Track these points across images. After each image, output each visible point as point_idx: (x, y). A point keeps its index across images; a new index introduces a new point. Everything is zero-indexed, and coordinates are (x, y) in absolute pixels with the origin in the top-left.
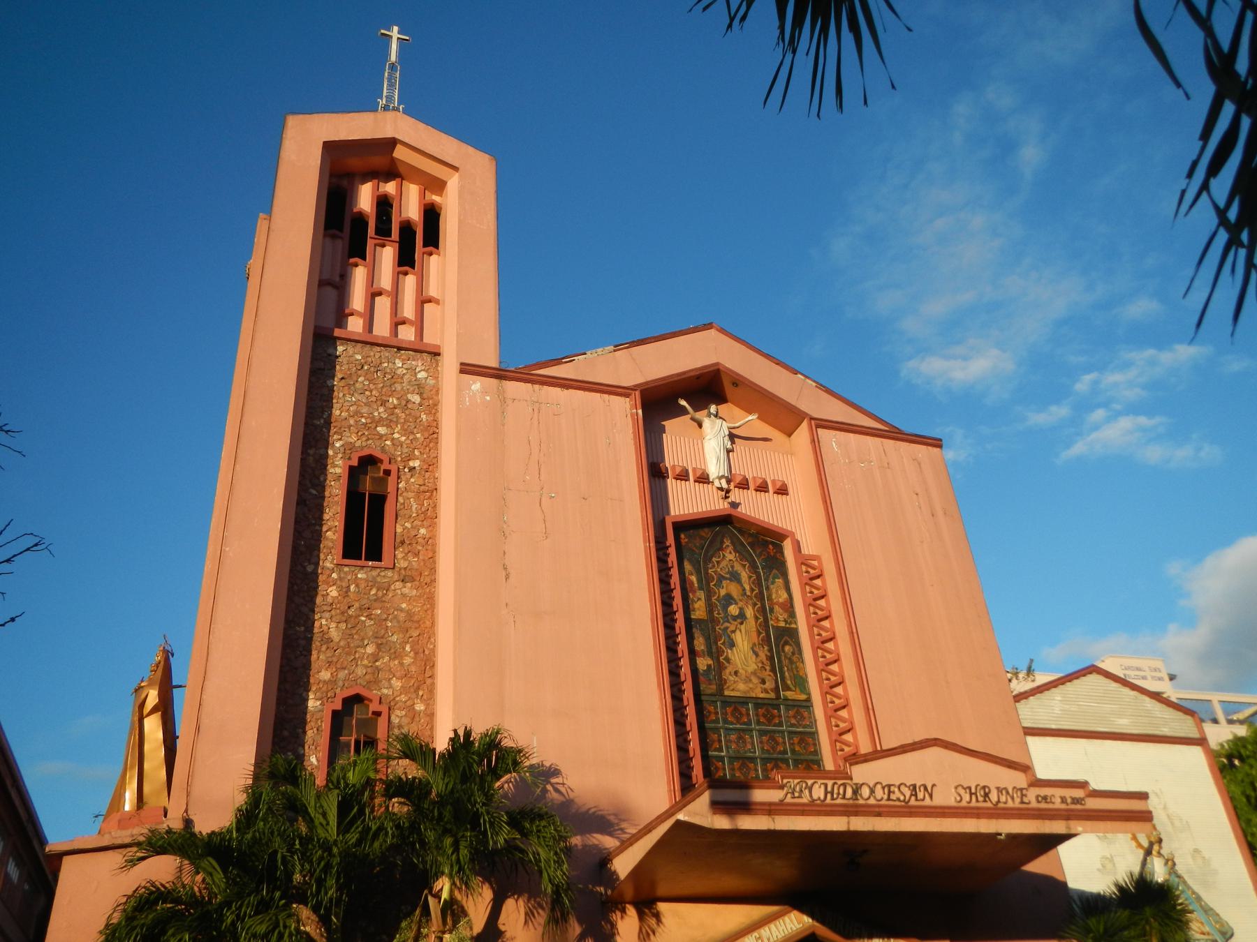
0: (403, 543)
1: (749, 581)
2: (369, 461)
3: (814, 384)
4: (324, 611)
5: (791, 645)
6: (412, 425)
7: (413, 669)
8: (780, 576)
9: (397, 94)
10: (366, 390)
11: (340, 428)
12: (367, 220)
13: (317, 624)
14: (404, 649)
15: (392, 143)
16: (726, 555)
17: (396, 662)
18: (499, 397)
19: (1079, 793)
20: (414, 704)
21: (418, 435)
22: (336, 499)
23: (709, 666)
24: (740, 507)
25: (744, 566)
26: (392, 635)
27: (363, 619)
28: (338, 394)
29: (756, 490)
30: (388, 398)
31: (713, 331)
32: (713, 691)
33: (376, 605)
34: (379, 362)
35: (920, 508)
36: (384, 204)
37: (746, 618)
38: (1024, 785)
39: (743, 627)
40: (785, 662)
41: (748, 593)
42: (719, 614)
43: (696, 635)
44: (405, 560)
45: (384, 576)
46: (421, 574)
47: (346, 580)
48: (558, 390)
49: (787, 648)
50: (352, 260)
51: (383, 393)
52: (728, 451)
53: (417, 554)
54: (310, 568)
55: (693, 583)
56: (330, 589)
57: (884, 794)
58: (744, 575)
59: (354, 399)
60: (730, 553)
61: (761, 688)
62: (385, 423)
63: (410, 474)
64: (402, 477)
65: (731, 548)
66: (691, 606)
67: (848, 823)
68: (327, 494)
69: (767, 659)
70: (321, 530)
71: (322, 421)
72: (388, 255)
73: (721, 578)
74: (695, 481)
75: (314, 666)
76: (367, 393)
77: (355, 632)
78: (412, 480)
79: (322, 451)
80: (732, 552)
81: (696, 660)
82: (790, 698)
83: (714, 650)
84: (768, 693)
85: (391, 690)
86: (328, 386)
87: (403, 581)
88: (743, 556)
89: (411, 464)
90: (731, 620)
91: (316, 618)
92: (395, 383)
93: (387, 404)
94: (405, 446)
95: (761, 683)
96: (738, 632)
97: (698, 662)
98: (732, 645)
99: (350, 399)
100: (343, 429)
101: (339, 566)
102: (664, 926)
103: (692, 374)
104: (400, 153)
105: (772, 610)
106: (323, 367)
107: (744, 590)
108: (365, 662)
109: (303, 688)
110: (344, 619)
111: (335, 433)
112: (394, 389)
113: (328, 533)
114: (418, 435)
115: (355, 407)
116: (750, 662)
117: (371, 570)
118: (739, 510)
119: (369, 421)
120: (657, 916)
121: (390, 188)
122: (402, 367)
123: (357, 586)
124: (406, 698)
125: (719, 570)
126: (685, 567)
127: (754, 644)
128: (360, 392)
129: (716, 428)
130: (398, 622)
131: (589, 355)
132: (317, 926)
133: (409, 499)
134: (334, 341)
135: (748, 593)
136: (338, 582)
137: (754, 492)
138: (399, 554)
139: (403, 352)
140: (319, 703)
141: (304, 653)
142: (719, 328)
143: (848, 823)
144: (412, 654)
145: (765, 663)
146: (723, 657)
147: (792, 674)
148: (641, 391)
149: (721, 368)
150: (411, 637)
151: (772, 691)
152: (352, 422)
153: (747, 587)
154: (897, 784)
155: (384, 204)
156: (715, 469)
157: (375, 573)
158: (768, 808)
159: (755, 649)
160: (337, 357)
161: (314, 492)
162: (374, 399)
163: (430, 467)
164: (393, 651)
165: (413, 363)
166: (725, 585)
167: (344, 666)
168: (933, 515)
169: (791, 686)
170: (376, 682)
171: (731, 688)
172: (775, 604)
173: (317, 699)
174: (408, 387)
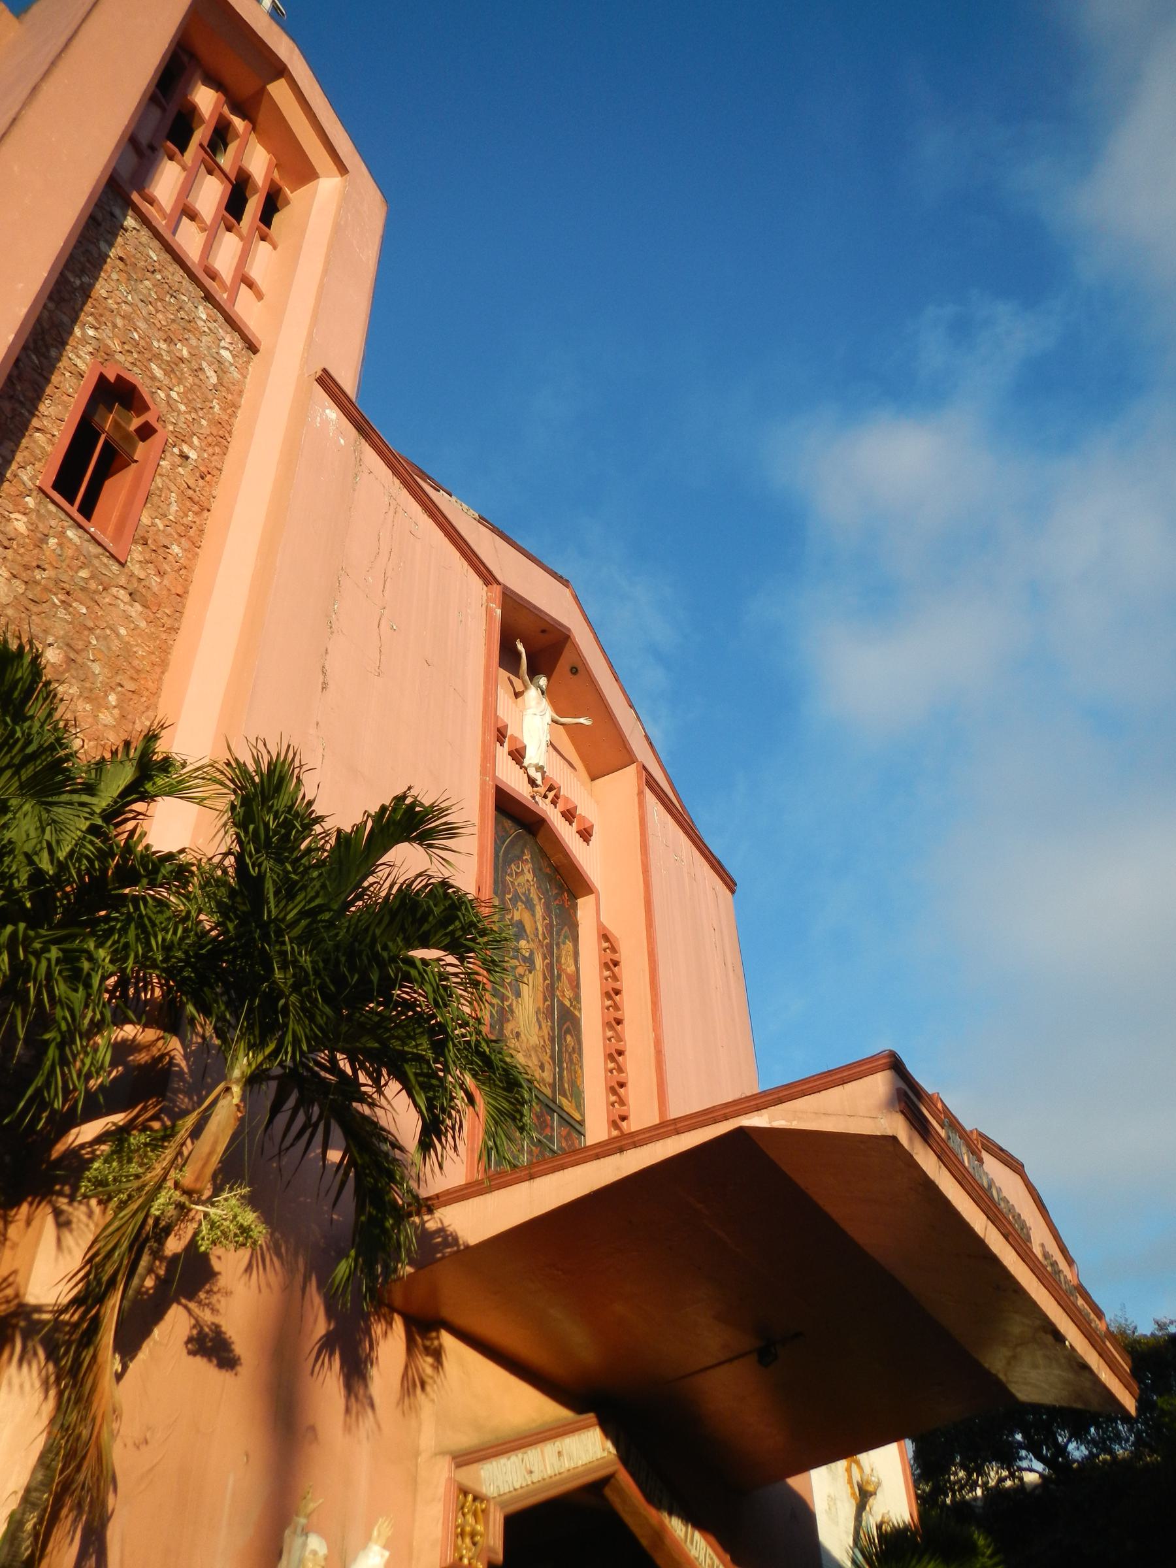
12: (194, 125)
14: (106, 696)
15: (280, 70)
17: (88, 707)
21: (204, 422)
25: (540, 899)
30: (177, 341)
33: (81, 595)
40: (565, 1056)
45: (105, 565)
48: (420, 509)
59: (130, 298)
71: (78, 282)
87: (131, 594)
89: (185, 448)
93: (172, 345)
101: (41, 495)
104: (278, 90)
113: (38, 434)
119: (142, 343)
120: (437, 1354)
121: (238, 123)
123: (60, 545)
128: (141, 297)
131: (454, 499)
136: (34, 516)
144: (116, 712)
150: (122, 686)
152: (119, 322)
163: (209, 476)
166: (520, 908)
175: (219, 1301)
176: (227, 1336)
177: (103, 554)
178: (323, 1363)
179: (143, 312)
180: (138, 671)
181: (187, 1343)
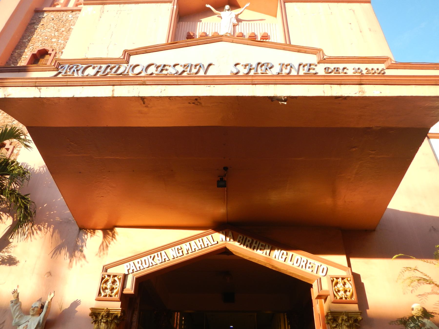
18: (101, 11)
34: (61, 17)
52: (234, 26)
62: (56, 37)
67: (113, 91)
76: (52, 28)
79: (22, 51)
94: (62, 44)
99: (43, 31)
102: (116, 240)
106: (35, 22)
111: (31, 43)
115: (44, 34)
139: (75, 12)
143: (113, 91)
152: (41, 39)
154: (172, 64)
160: (43, 18)
162: (54, 30)
168: (361, 32)
175: (11, 249)
178: (56, 254)
179: (49, 31)
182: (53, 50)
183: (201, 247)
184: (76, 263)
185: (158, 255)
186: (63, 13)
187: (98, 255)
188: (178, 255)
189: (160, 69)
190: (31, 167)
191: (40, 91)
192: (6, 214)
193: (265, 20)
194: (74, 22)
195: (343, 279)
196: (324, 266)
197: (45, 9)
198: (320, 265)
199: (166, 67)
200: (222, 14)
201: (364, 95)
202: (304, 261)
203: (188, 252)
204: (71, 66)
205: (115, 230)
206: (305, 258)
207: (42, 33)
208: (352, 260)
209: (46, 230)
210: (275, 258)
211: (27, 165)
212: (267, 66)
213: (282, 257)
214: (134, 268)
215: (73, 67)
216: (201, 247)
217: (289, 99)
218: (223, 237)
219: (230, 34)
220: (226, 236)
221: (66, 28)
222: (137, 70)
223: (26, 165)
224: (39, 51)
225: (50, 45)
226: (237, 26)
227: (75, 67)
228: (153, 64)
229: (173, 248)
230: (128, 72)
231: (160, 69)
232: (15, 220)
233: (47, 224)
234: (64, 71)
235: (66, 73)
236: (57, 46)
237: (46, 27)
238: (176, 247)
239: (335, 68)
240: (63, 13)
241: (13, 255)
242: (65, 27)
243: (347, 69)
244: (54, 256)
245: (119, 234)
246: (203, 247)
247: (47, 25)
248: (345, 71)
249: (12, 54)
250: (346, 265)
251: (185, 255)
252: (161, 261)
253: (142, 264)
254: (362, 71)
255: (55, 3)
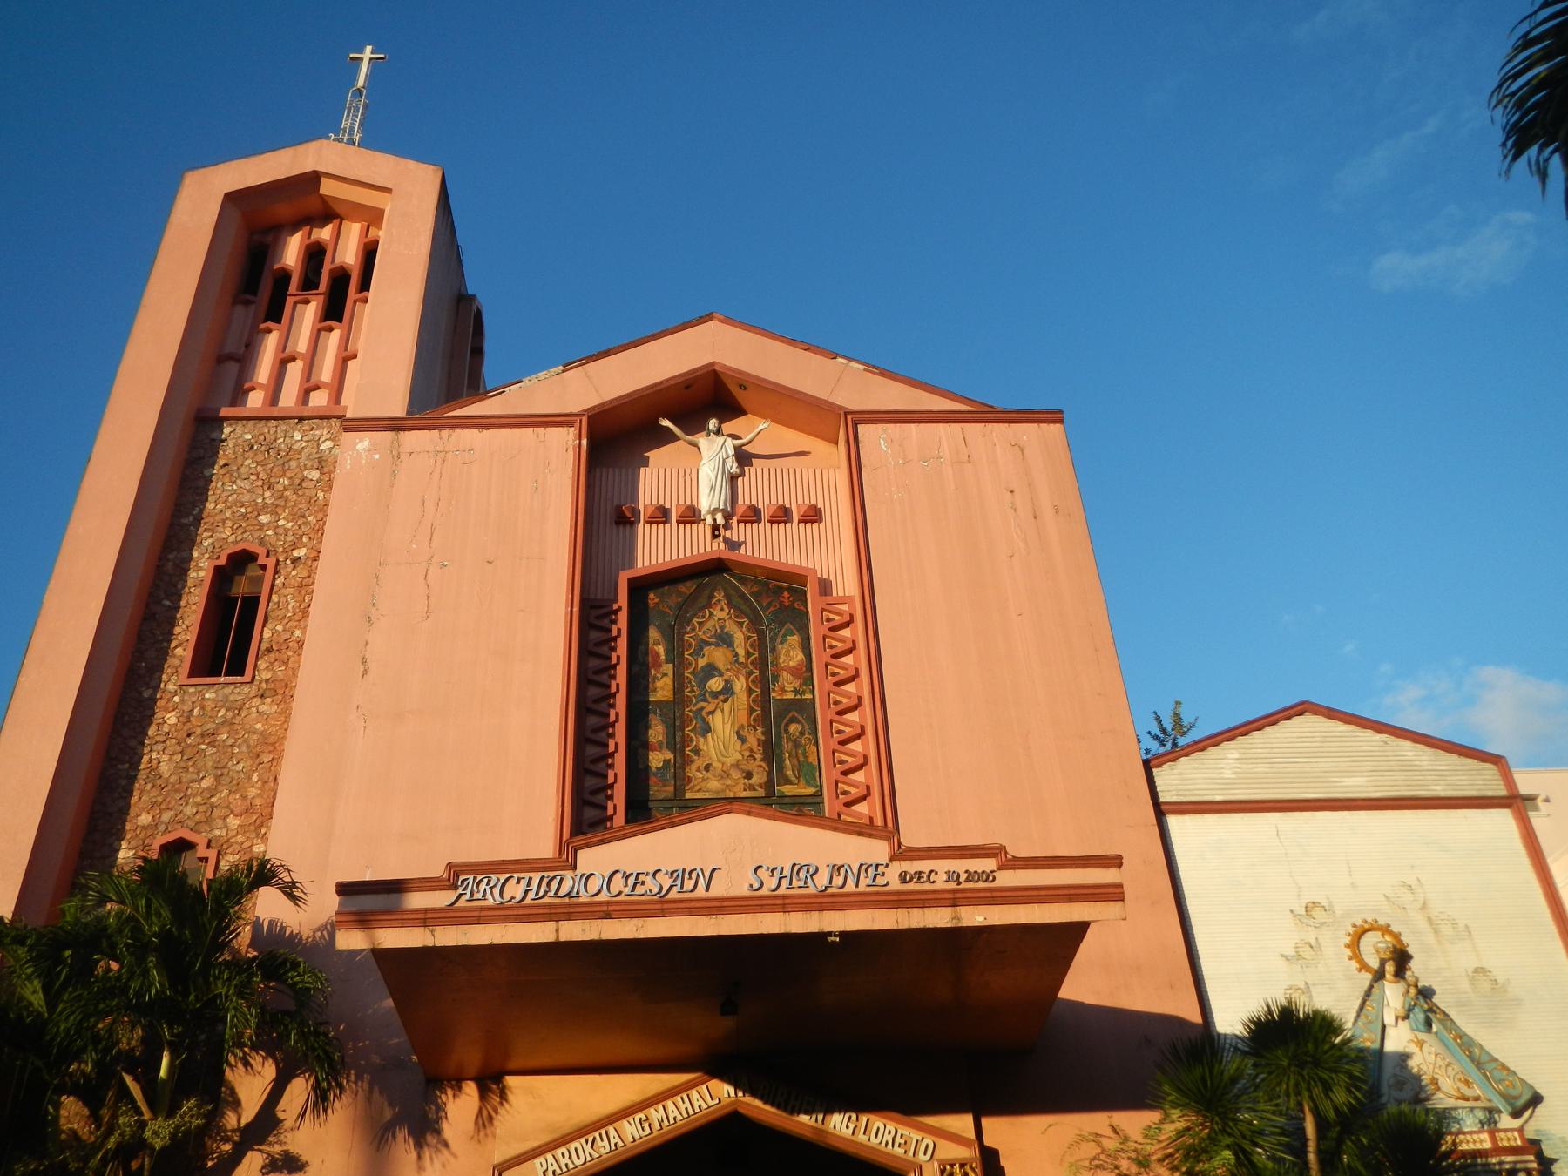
0: (270, 650)
1: (746, 642)
2: (241, 560)
3: (862, 367)
4: (157, 742)
5: (798, 722)
6: (304, 507)
7: (258, 802)
8: (794, 630)
9: (357, 124)
10: (252, 474)
11: (213, 523)
13: (145, 759)
14: (250, 778)
15: (314, 178)
16: (715, 613)
19: (988, 864)
20: (253, 845)
21: (310, 518)
22: (194, 607)
23: (666, 762)
24: (743, 547)
25: (741, 625)
26: (238, 763)
27: (203, 747)
28: (216, 485)
29: (772, 522)
31: (712, 324)
32: (668, 794)
34: (273, 438)
35: (1015, 510)
36: (315, 255)
37: (733, 693)
38: (885, 860)
39: (726, 706)
41: (742, 660)
42: (692, 691)
43: (653, 723)
44: (269, 670)
46: (286, 685)
47: (190, 703)
49: (793, 728)
50: (263, 326)
51: (273, 475)
52: (733, 479)
53: (286, 662)
54: (146, 694)
55: (658, 655)
56: (168, 716)
57: (626, 886)
58: (739, 637)
59: (235, 487)
60: (722, 609)
61: (744, 784)
62: (269, 510)
63: (292, 566)
64: (282, 571)
65: (723, 603)
66: (651, 686)
67: (557, 930)
68: (183, 603)
69: (759, 745)
70: (169, 647)
71: (191, 519)
72: (309, 313)
73: (703, 644)
74: (678, 522)
75: (133, 811)
76: (253, 477)
77: (190, 764)
78: (294, 573)
79: (185, 554)
80: (725, 607)
81: (648, 755)
82: (787, 794)
83: (678, 735)
84: (755, 790)
85: (225, 831)
86: (205, 477)
87: (262, 696)
88: (741, 610)
89: (295, 554)
90: (710, 699)
91: (145, 752)
92: (290, 460)
94: (290, 533)
95: (744, 778)
96: (718, 712)
97: (650, 757)
98: (706, 730)
99: (230, 488)
100: (216, 524)
101: (184, 688)
102: (511, 1105)
103: (672, 382)
104: (327, 188)
105: (776, 678)
107: (737, 655)
108: (199, 799)
109: (114, 837)
110: (179, 749)
111: (205, 530)
112: (287, 467)
113: (177, 650)
114: (310, 518)
115: (235, 496)
116: (731, 749)
117: (223, 688)
118: (742, 551)
119: (249, 510)
121: (325, 234)
122: (302, 440)
123: (203, 708)
124: (243, 839)
125: (700, 634)
126: (650, 635)
127: (742, 727)
128: (243, 477)
129: (715, 448)
130: (248, 746)
131: (526, 380)
132: (86, 1123)
133: (286, 596)
134: (219, 422)
135: (742, 660)
137: (768, 525)
138: (262, 664)
139: (306, 422)
140: (131, 853)
141: (124, 794)
142: (722, 317)
143: (557, 930)
145: (755, 750)
146: (690, 748)
147: (796, 763)
148: (589, 417)
149: (717, 368)
151: (761, 787)
152: (228, 514)
153: (741, 652)
154: (651, 871)
155: (315, 255)
156: (708, 500)
157: (227, 690)
158: (422, 916)
159: (742, 733)
160: (223, 441)
161: (167, 603)
162: (260, 483)
164: (235, 782)
165: (317, 432)
166: (706, 653)
167: (170, 806)
168: (1035, 518)
169: (793, 778)
170: (209, 821)
171: (697, 788)
172: (782, 669)
173: (130, 849)
174: (306, 462)
175: (286, 1137)
176: (295, 1154)
177: (236, 688)
178: (387, 1140)
179: (247, 488)
180: (273, 744)
181: (261, 1171)
182: (268, 556)
183: (688, 1113)
184: (431, 1159)
185: (600, 1135)
186: (276, 427)
187: (476, 1138)
188: (643, 1134)
189: (631, 881)
190: (292, 932)
191: (433, 935)
192: (258, 1053)
193: (809, 453)
194: (309, 456)
195: (962, 1166)
196: (929, 1141)
197: (222, 414)
198: (920, 1139)
199: (641, 878)
200: (702, 440)
201: (960, 925)
202: (889, 1133)
203: (660, 1125)
204: (479, 877)
205: (505, 1083)
206: (891, 1127)
207: (229, 496)
208: (987, 1122)
209: (354, 1086)
210: (835, 1127)
211: (282, 924)
212: (808, 872)
213: (847, 1127)
214: (556, 1167)
215: (482, 880)
216: (688, 1113)
217: (843, 934)
218: (732, 1091)
219: (723, 511)
220: (736, 1088)
221: (290, 478)
222: (594, 885)
223: (279, 924)
224: (231, 556)
225: (256, 534)
226: (740, 480)
227: (486, 880)
228: (617, 871)
229: (631, 1119)
230: (578, 893)
231: (631, 881)
232: (281, 1066)
233: (352, 1072)
234: (468, 892)
235: (472, 895)
236: (278, 540)
237: (236, 474)
238: (637, 1117)
239: (916, 873)
240: (276, 427)
241: (294, 1148)
242: (289, 474)
243: (936, 873)
244: (381, 1146)
245: (513, 1090)
246: (691, 1112)
247: (238, 469)
248: (933, 877)
249: (158, 566)
250: (972, 1135)
251: (656, 1133)
252: (608, 1150)
253: (570, 1157)
254: (959, 876)
255: (246, 386)
